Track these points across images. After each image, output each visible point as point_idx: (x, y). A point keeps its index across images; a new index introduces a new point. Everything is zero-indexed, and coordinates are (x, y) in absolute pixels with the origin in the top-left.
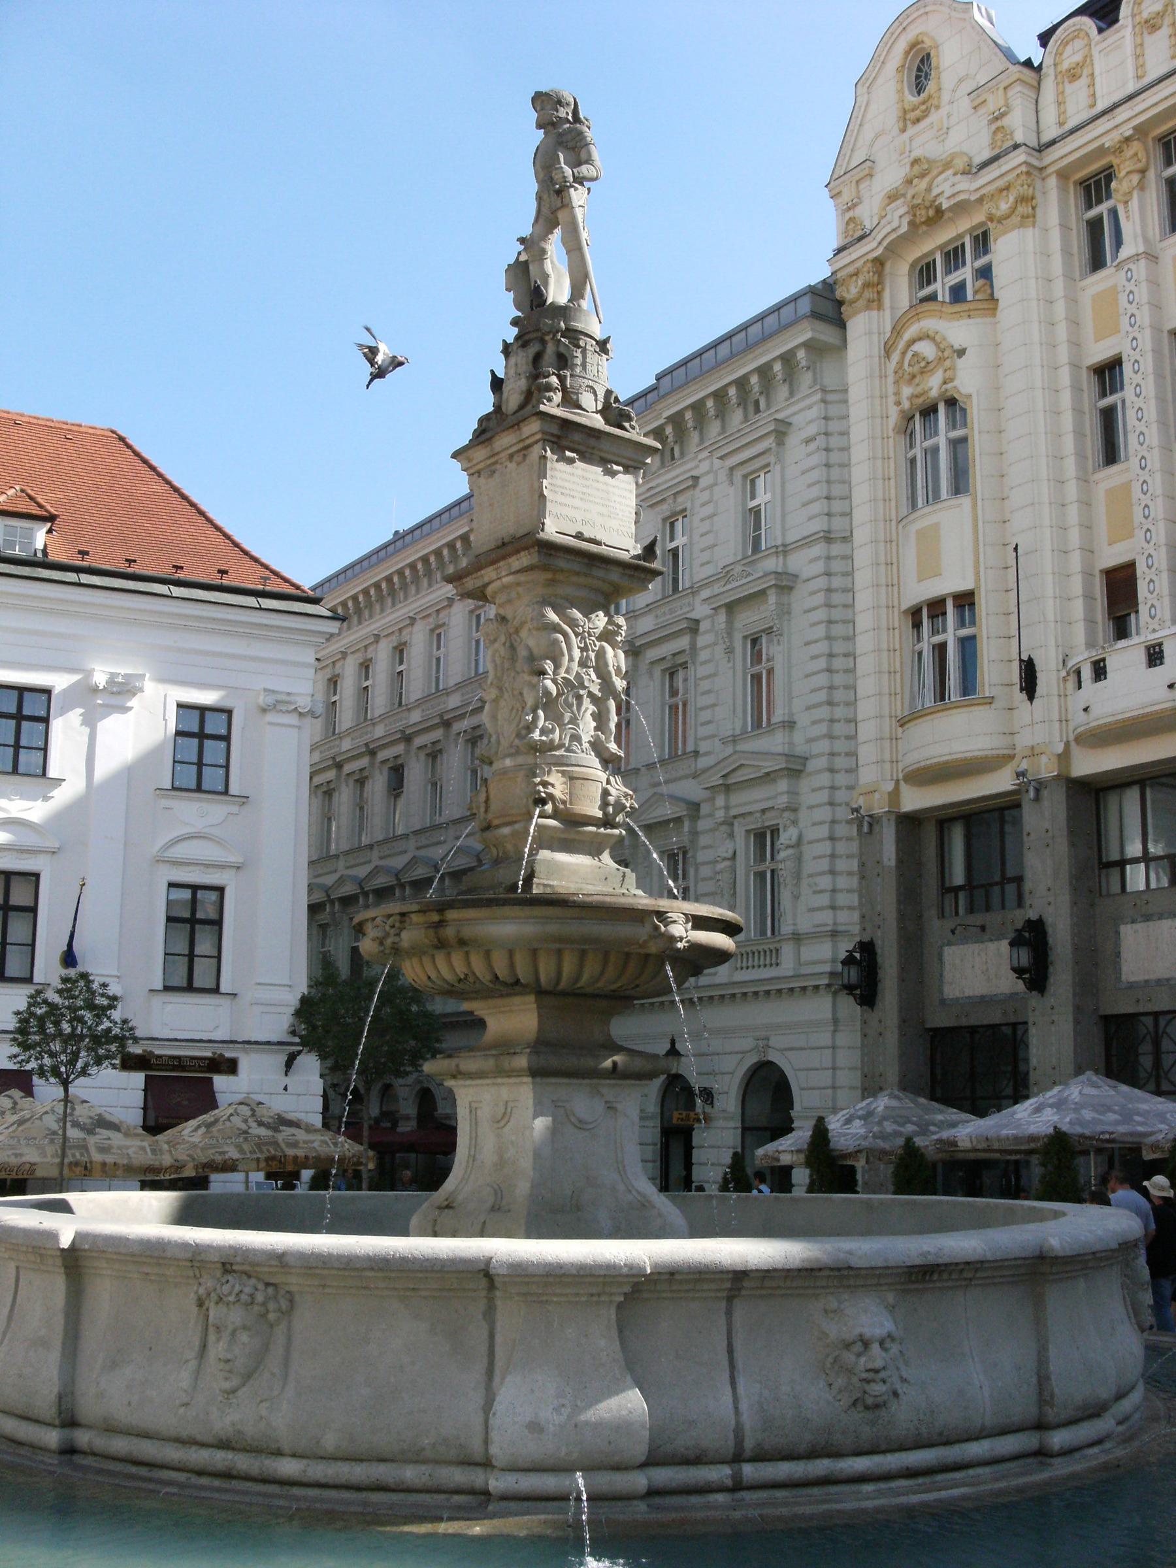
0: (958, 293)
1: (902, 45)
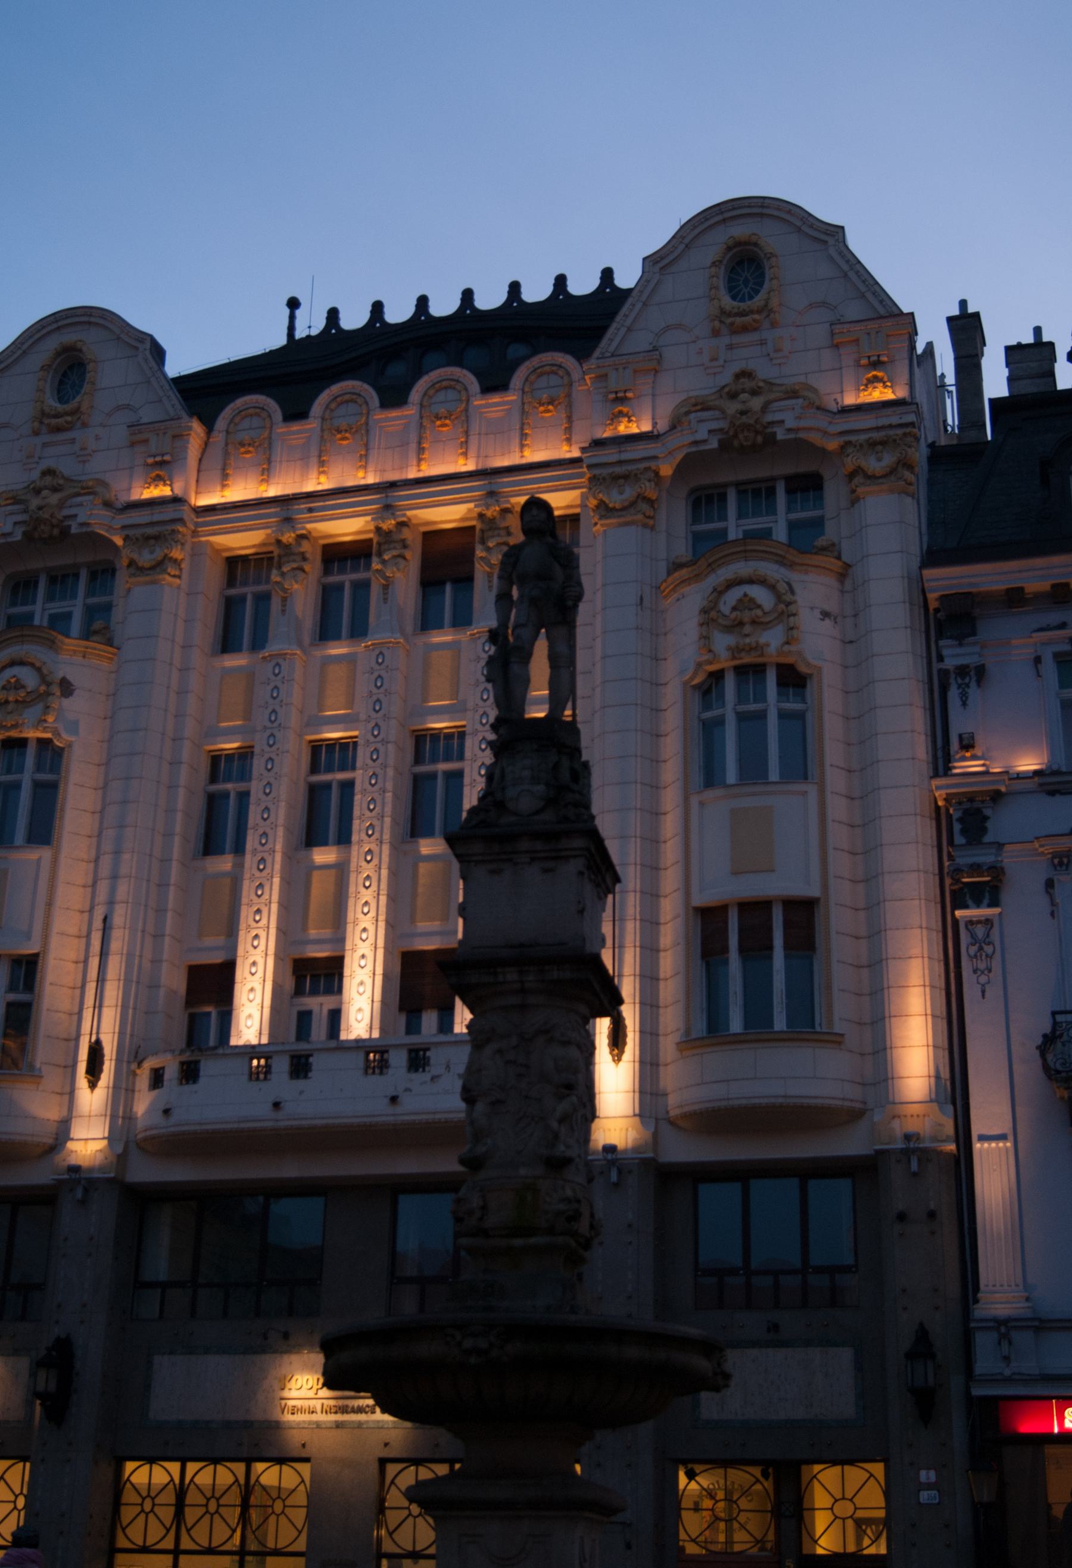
1: (52, 344)
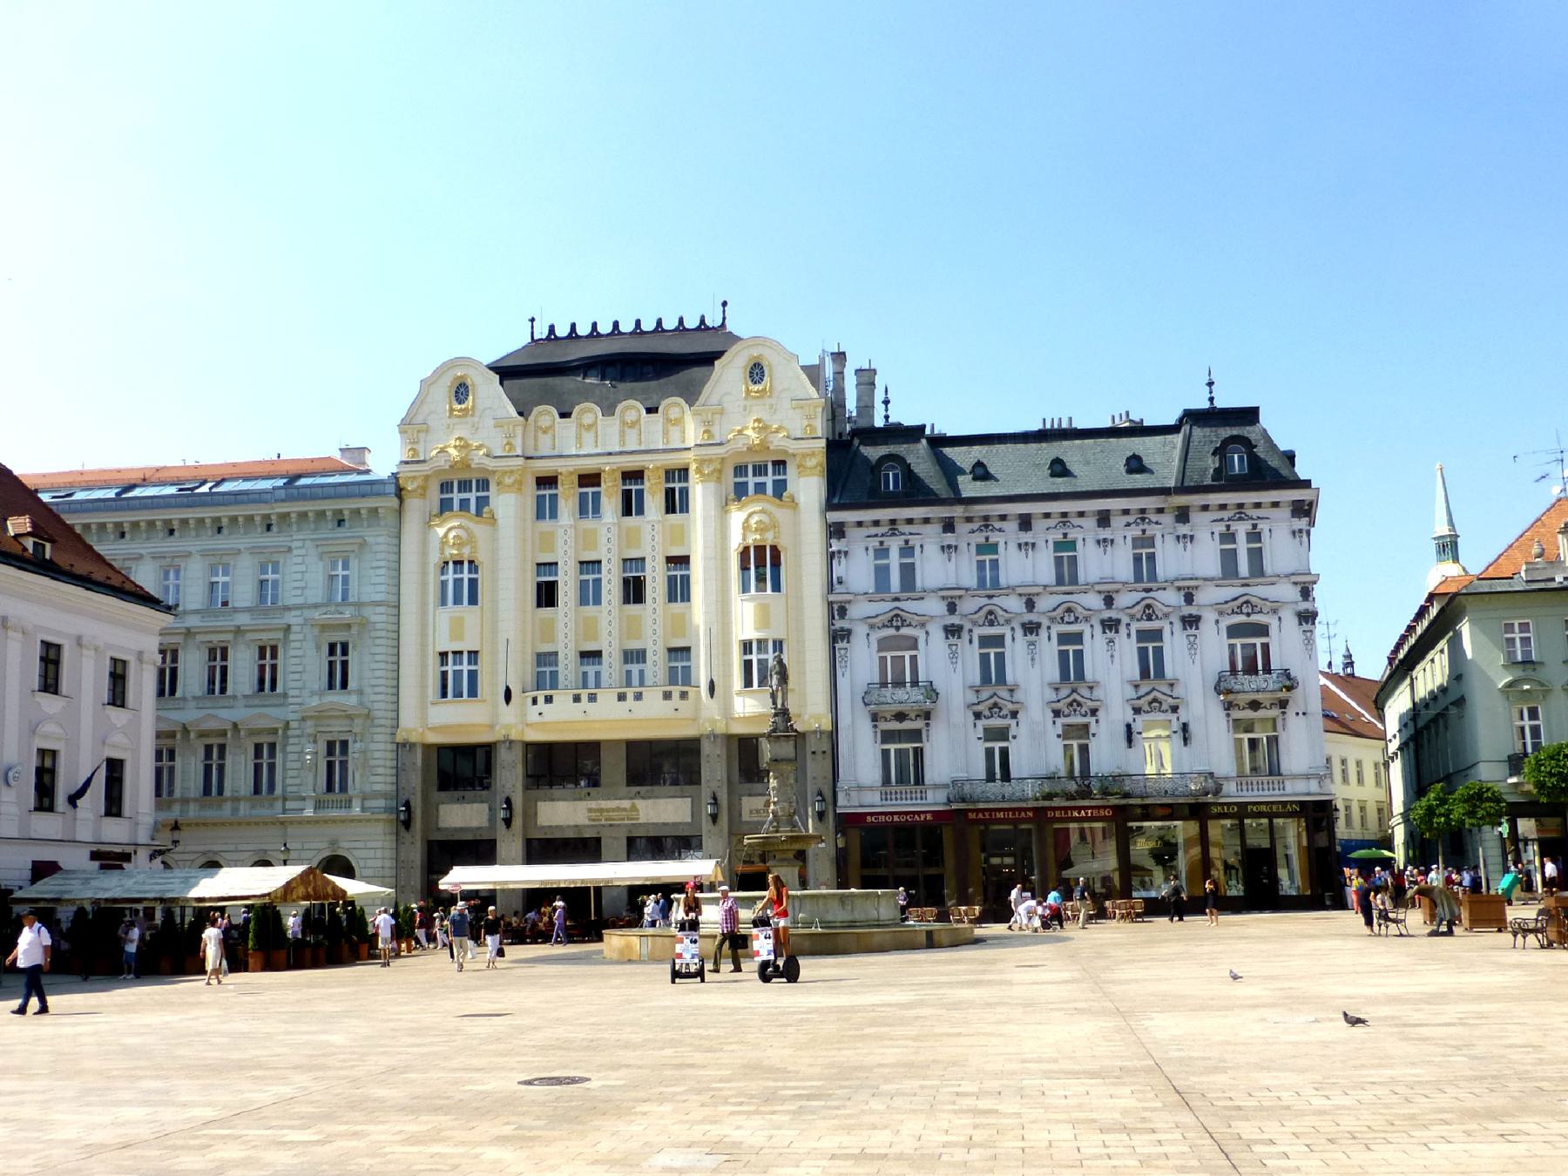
0: (464, 504)
